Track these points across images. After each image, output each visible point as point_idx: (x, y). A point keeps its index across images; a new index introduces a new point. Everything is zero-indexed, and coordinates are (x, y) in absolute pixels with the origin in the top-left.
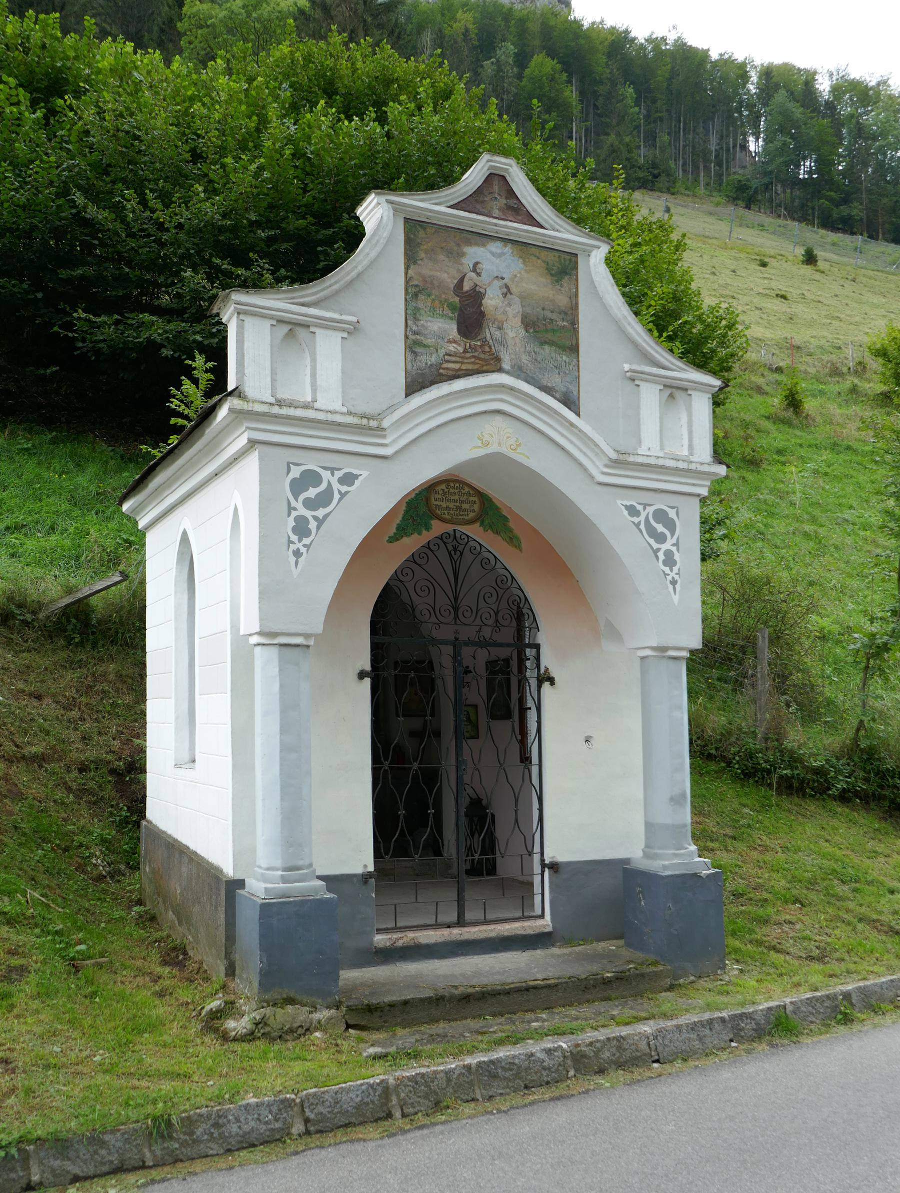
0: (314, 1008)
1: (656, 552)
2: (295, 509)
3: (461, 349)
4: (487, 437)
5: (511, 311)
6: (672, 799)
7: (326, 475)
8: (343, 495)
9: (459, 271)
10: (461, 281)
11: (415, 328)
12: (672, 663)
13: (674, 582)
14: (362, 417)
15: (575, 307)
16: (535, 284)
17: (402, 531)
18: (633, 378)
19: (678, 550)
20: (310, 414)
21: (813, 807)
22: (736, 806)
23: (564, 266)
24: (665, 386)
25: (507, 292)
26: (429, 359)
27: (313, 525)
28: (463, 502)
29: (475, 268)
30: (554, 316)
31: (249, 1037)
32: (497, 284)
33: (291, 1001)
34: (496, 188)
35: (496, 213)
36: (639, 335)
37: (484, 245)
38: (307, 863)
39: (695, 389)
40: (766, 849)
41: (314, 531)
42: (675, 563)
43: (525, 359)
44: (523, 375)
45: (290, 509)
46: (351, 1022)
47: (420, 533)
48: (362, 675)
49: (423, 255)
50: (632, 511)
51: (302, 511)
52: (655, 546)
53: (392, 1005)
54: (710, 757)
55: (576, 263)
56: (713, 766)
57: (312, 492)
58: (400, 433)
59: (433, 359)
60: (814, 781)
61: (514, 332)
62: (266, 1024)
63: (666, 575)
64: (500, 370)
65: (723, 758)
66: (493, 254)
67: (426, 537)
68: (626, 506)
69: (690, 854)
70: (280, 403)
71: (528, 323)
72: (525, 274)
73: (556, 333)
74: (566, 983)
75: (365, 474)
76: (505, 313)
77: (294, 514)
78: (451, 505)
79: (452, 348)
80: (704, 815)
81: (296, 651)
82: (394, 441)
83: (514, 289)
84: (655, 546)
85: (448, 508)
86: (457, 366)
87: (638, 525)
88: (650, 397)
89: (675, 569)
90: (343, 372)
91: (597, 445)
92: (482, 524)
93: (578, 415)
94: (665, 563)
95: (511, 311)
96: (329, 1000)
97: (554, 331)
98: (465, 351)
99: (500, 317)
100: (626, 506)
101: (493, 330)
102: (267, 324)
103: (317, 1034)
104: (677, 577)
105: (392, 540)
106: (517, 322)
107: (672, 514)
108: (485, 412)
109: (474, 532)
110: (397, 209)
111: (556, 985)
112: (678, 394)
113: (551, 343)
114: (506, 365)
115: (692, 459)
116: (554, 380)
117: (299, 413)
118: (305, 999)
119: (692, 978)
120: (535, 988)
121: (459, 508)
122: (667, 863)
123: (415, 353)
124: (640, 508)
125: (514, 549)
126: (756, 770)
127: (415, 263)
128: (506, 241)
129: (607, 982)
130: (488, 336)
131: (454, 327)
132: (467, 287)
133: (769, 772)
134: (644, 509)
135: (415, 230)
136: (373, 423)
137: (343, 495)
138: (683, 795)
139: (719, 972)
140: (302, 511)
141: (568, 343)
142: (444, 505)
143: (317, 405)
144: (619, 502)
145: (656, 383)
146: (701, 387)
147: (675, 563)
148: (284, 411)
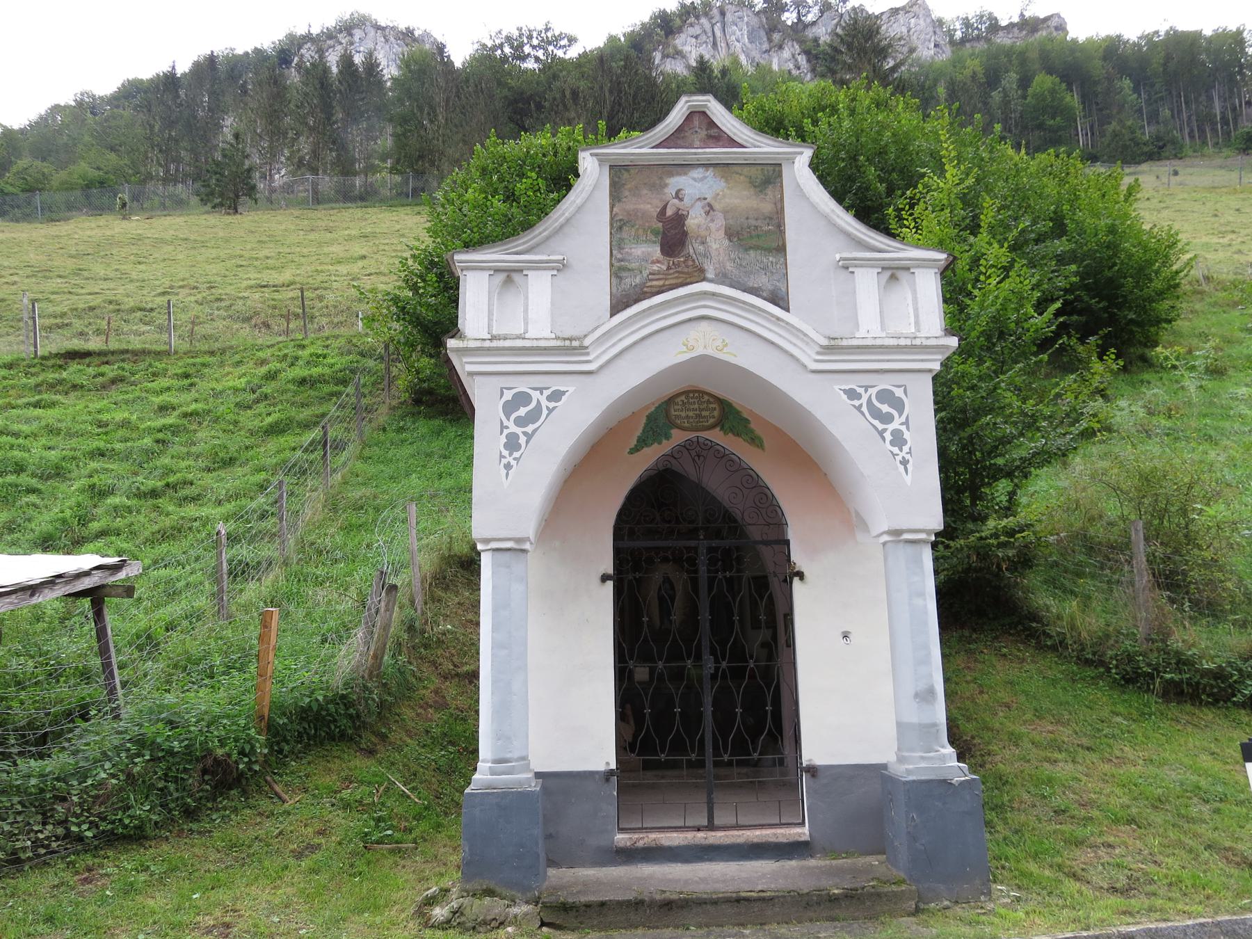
0: (513, 902)
1: (881, 433)
2: (507, 427)
3: (664, 268)
4: (692, 343)
5: (712, 225)
6: (917, 695)
7: (535, 395)
8: (550, 411)
9: (661, 200)
10: (665, 208)
11: (619, 256)
12: (910, 549)
13: (904, 462)
14: (565, 339)
15: (780, 211)
16: (740, 199)
17: (643, 442)
18: (846, 266)
19: (908, 429)
20: (519, 343)
21: (1211, 716)
22: (1105, 713)
23: (768, 177)
24: (883, 268)
25: (710, 209)
27: (522, 440)
28: (701, 410)
29: (678, 196)
30: (759, 223)
31: (446, 925)
32: (699, 204)
33: (490, 893)
34: (696, 123)
35: (697, 143)
36: (849, 224)
37: (685, 174)
38: (516, 755)
39: (918, 267)
40: (1122, 761)
41: (523, 445)
42: (905, 442)
43: (729, 266)
44: (728, 281)
45: (503, 427)
46: (546, 920)
47: (660, 443)
48: (604, 578)
49: (627, 193)
50: (852, 394)
51: (513, 428)
52: (881, 427)
53: (588, 906)
54: (1088, 662)
55: (780, 172)
56: (1090, 672)
57: (522, 411)
58: (604, 348)
59: (638, 280)
60: (1212, 687)
61: (717, 244)
62: (462, 914)
63: (894, 455)
64: (704, 279)
65: (1102, 663)
66: (694, 179)
67: (665, 447)
68: (844, 391)
69: (943, 758)
70: (493, 338)
72: (727, 192)
73: (762, 239)
74: (784, 897)
75: (571, 389)
76: (708, 229)
77: (506, 432)
78: (691, 414)
79: (655, 268)
80: (1063, 724)
81: (507, 555)
82: (598, 357)
83: (716, 206)
84: (881, 427)
85: (687, 417)
86: (661, 283)
87: (859, 408)
88: (867, 282)
89: (906, 449)
90: (553, 304)
91: (805, 335)
92: (722, 429)
93: (788, 310)
94: (892, 443)
95: (712, 225)
96: (529, 895)
97: (758, 236)
98: (669, 268)
99: (703, 233)
100: (844, 391)
101: (696, 245)
102: (486, 274)
103: (510, 929)
104: (908, 457)
105: (633, 451)
107: (899, 393)
108: (690, 320)
109: (716, 436)
110: (602, 159)
111: (772, 899)
112: (900, 274)
113: (756, 248)
114: (710, 275)
115: (918, 334)
116: (762, 280)
117: (508, 343)
118: (505, 892)
119: (946, 903)
120: (747, 899)
121: (699, 416)
122: (911, 767)
123: (621, 278)
124: (861, 390)
125: (756, 449)
126: (1139, 675)
127: (619, 201)
128: (706, 166)
129: (833, 900)
130: (691, 251)
131: (658, 249)
132: (669, 212)
133: (1151, 676)
134: (866, 391)
135: (619, 173)
136: (576, 344)
137: (550, 411)
138: (931, 691)
139: (982, 898)
140: (513, 428)
141: (774, 245)
142: (683, 414)
143: (527, 336)
144: (836, 387)
145: (873, 267)
146: (924, 264)
147: (905, 442)
148: (495, 344)
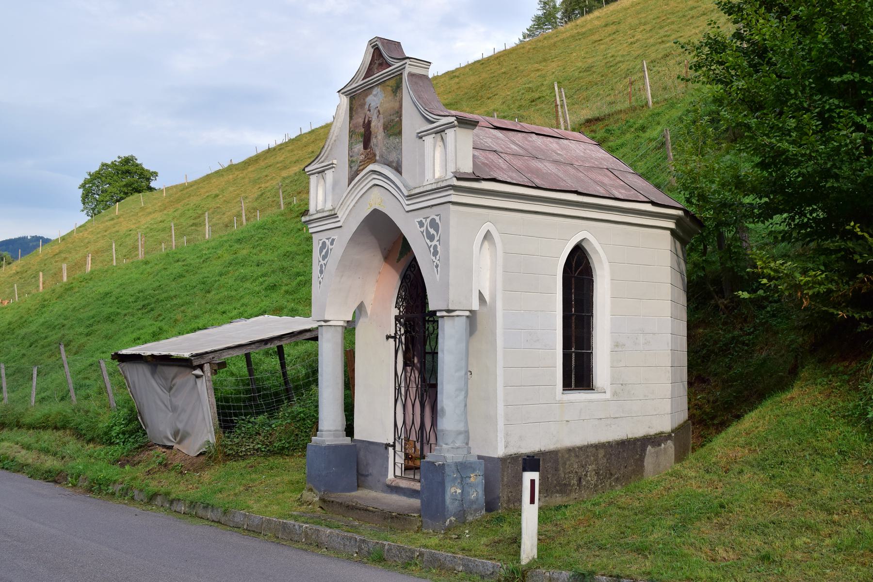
26: (355, 168)
39: (448, 128)
50: (421, 224)
64: (375, 161)
70: (318, 212)
71: (386, 128)
87: (422, 233)
106: (381, 129)
116: (393, 157)
